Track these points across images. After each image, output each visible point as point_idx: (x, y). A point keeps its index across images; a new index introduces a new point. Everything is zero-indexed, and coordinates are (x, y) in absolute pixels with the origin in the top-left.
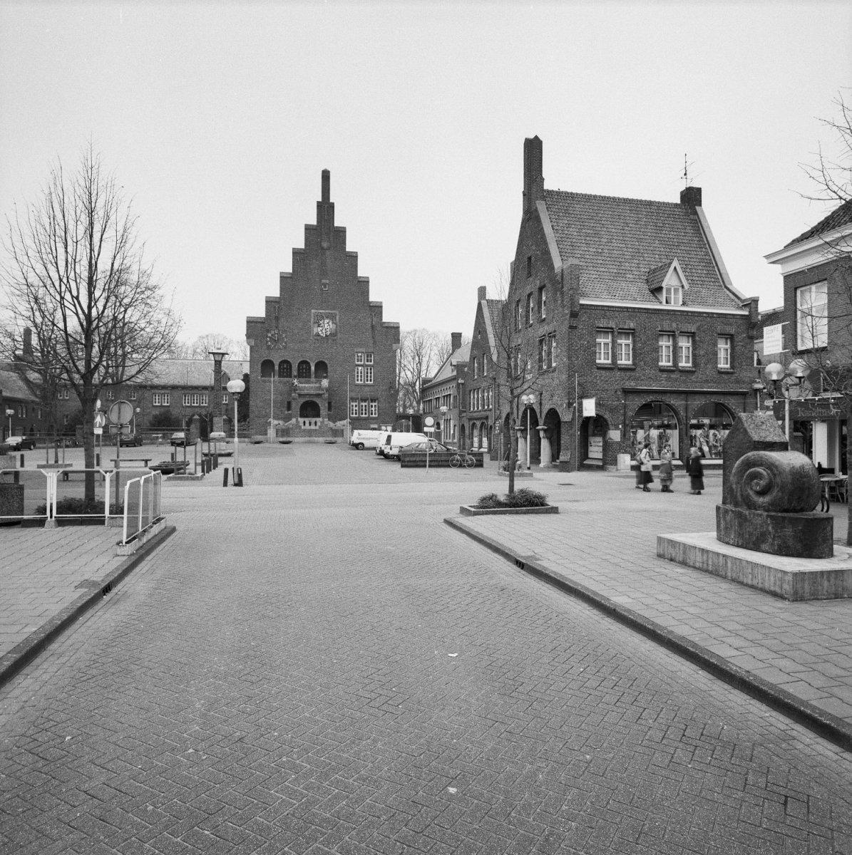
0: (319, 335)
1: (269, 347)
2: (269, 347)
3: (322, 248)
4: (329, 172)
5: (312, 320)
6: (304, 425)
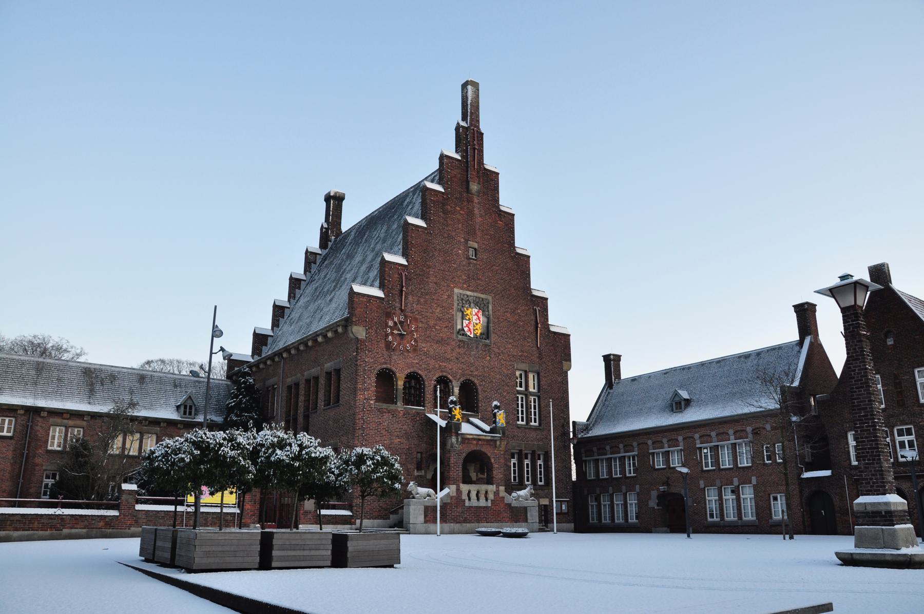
0: (466, 335)
1: (388, 346)
5: (455, 305)
6: (469, 499)
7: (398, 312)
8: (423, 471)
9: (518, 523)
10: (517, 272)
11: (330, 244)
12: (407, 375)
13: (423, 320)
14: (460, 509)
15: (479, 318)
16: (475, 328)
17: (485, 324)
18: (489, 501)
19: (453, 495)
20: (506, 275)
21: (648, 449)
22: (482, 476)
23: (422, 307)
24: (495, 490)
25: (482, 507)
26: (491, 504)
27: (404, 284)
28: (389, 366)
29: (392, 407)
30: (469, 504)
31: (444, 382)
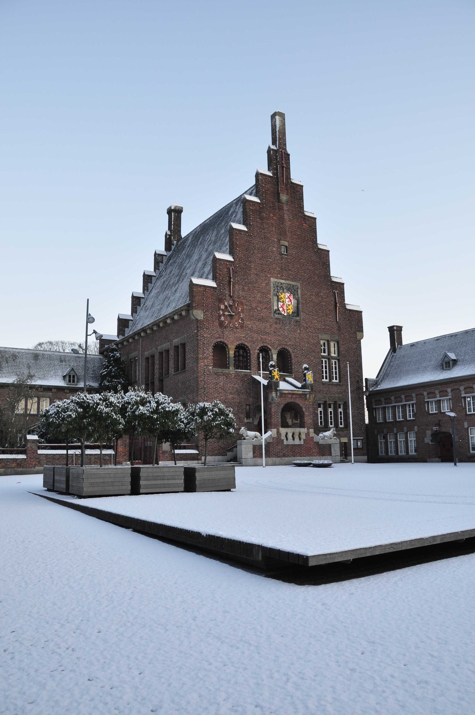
0: (281, 314)
1: (221, 324)
2: (221, 324)
6: (287, 439)
7: (228, 298)
8: (251, 419)
9: (324, 457)
11: (173, 247)
12: (237, 346)
13: (247, 303)
14: (280, 447)
15: (291, 301)
16: (287, 308)
17: (296, 305)
18: (302, 440)
19: (275, 436)
21: (424, 399)
22: (296, 422)
23: (246, 293)
24: (306, 432)
25: (296, 445)
27: (231, 276)
28: (222, 340)
29: (226, 371)
30: (287, 442)
31: (265, 351)
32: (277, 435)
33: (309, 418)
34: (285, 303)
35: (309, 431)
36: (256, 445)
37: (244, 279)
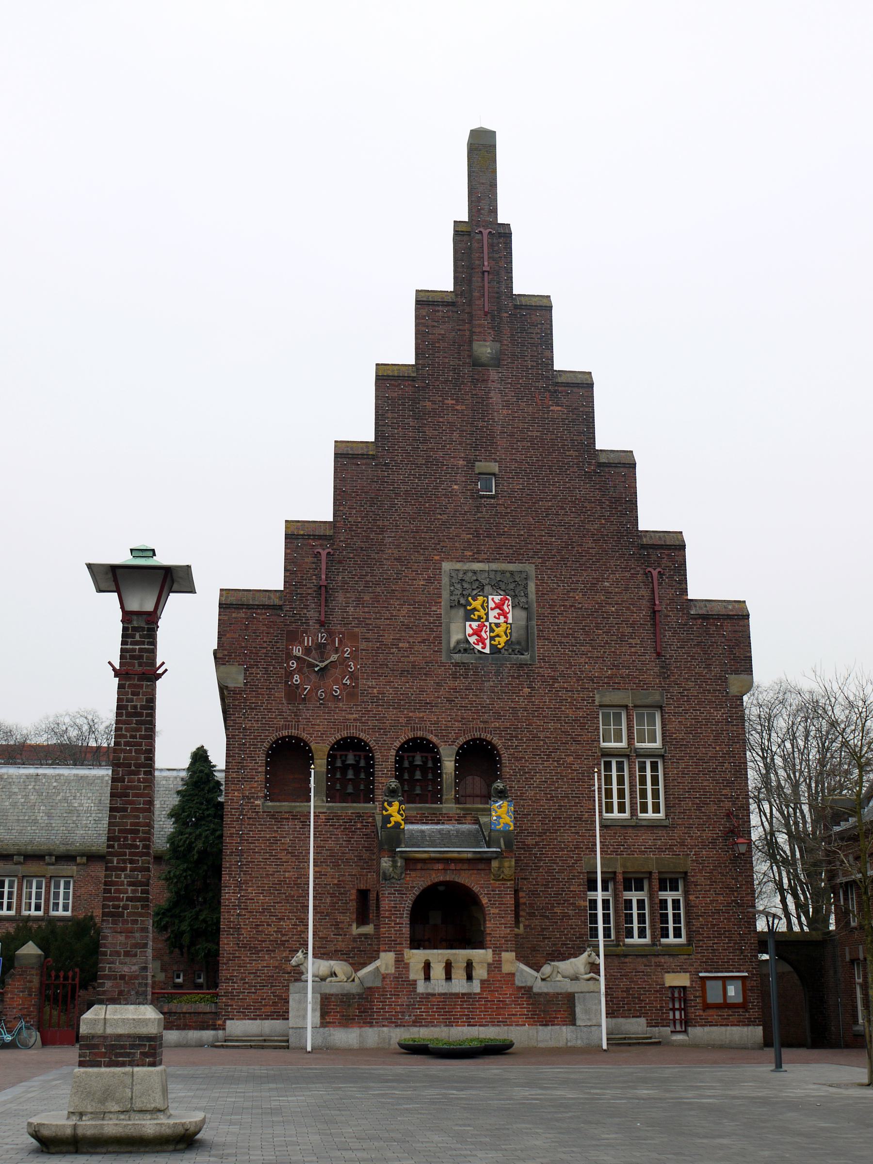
1: (293, 694)
3: (476, 363)
4: (492, 134)
5: (445, 594)
6: (427, 978)
7: (313, 626)
9: (550, 1028)
10: (601, 503)
13: (370, 635)
14: (404, 1000)
16: (492, 634)
19: (389, 972)
20: (572, 515)
23: (366, 610)
24: (490, 961)
25: (457, 994)
26: (481, 988)
28: (294, 732)
30: (427, 988)
32: (396, 968)
33: (500, 924)
34: (487, 620)
35: (501, 957)
36: (332, 995)
37: (362, 577)
